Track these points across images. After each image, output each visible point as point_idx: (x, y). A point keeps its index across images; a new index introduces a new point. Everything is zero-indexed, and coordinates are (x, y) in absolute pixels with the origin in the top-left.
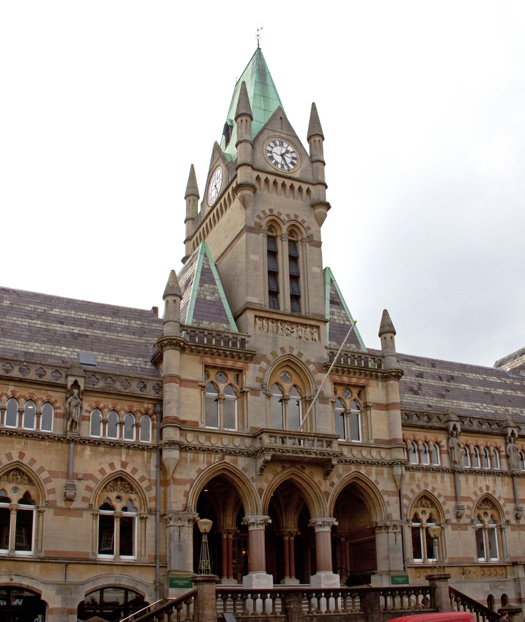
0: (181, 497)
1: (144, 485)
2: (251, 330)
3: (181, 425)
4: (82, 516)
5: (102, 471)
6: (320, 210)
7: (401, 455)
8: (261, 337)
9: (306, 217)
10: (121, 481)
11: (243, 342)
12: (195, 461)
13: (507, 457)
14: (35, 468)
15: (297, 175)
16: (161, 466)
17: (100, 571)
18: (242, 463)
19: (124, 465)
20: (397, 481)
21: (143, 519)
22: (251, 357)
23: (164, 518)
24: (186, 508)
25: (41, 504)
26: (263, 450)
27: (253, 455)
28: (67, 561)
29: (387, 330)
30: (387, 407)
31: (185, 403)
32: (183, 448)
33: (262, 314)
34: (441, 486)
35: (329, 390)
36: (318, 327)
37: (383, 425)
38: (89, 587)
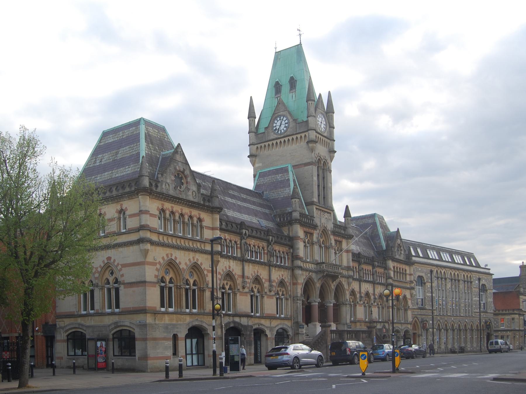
0: (299, 290)
1: (288, 284)
2: (315, 215)
3: (300, 259)
4: (247, 296)
5: (277, 278)
6: (332, 155)
7: (351, 273)
8: (320, 219)
10: (282, 283)
11: (313, 220)
12: (303, 274)
13: (373, 274)
14: (261, 277)
16: (294, 276)
17: (279, 322)
18: (314, 276)
19: (282, 275)
20: (349, 284)
21: (287, 299)
22: (315, 227)
23: (295, 299)
24: (301, 295)
25: (264, 293)
26: (323, 271)
27: (316, 272)
28: (271, 318)
30: (347, 251)
31: (301, 249)
33: (318, 207)
36: (330, 213)
37: (346, 260)
38: (277, 328)
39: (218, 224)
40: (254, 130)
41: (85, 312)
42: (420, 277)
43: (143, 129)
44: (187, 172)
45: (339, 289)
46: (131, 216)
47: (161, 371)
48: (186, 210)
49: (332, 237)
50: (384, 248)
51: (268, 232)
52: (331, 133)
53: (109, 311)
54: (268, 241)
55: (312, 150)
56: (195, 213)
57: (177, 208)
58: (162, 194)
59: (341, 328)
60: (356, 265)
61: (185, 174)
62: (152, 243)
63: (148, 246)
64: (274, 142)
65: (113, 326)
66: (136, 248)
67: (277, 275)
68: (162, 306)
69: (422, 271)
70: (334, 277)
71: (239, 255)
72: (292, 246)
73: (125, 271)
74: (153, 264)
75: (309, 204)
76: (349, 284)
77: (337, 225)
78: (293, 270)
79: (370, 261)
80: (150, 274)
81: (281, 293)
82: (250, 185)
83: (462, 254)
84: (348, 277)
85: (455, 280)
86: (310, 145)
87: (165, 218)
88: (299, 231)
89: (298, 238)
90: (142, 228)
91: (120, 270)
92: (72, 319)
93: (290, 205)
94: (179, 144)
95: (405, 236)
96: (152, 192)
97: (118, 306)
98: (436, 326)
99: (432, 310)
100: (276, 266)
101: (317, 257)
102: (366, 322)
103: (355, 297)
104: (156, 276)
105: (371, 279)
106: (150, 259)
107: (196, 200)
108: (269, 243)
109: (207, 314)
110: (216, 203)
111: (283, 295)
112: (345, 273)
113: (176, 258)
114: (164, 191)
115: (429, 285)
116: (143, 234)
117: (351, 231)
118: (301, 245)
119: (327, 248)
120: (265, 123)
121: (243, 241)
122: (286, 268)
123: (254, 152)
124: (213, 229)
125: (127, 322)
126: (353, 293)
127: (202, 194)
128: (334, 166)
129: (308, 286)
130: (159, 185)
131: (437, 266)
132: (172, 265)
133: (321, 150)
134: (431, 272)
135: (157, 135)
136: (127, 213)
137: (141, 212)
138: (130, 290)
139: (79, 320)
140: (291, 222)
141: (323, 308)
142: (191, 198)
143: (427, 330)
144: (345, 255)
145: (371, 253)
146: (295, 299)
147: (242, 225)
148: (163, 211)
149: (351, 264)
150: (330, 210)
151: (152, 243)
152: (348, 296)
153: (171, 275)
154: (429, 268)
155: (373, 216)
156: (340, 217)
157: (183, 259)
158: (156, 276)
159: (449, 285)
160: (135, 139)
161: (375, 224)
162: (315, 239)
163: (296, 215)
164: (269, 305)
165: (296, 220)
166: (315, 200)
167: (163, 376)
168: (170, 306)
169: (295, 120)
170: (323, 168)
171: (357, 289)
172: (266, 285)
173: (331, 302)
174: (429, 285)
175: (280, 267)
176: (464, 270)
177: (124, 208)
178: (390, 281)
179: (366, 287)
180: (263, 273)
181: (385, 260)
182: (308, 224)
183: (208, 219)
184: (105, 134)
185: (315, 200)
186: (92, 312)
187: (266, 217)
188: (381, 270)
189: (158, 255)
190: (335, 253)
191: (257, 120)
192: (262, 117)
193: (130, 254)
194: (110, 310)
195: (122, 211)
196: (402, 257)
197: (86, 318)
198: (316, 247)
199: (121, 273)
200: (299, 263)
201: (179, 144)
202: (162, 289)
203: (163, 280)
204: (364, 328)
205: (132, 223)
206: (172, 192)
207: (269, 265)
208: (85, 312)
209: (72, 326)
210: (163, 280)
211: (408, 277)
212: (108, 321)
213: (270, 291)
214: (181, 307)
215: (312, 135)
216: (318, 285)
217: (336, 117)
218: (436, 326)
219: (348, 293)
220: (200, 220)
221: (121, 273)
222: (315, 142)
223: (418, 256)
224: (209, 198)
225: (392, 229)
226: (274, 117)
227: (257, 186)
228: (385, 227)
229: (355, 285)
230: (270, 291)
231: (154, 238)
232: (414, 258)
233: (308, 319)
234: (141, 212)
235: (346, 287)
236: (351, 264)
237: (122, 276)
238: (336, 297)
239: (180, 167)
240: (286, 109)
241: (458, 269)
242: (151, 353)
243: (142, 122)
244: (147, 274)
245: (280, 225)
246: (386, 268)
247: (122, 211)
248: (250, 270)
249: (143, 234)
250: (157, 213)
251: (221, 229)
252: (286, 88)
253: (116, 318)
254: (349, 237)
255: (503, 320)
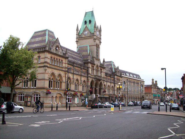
0: (89, 84)
8: (96, 62)
9: (99, 44)
10: (84, 81)
15: (99, 37)
16: (88, 79)
18: (94, 79)
20: (104, 82)
21: (86, 86)
22: (95, 65)
23: (87, 86)
26: (96, 78)
27: (94, 78)
29: (104, 61)
32: (90, 77)
34: (105, 83)
35: (100, 69)
37: (103, 75)
39: (67, 62)
40: (78, 34)
41: (24, 87)
42: (124, 81)
43: (47, 33)
44: (59, 46)
45: (101, 84)
46: (42, 58)
47: (50, 108)
48: (58, 58)
49: (99, 68)
50: (114, 72)
51: (81, 65)
52: (100, 37)
53: (32, 87)
54: (81, 68)
55: (95, 41)
56: (61, 58)
57: (56, 57)
58: (52, 52)
59: (101, 96)
60: (106, 77)
61: (58, 46)
62: (48, 67)
63: (46, 68)
64: (84, 38)
65: (33, 92)
66: (43, 68)
67: (83, 79)
68: (49, 87)
69: (125, 80)
70: (100, 80)
71: (72, 72)
72: (88, 70)
73: (39, 75)
74: (48, 74)
75: (93, 57)
76: (104, 82)
77: (101, 64)
78: (87, 77)
79: (110, 76)
80: (47, 76)
81: (84, 84)
82: (75, 50)
83: (136, 75)
84: (104, 80)
85: (134, 83)
86: (94, 40)
87: (52, 60)
88: (90, 65)
89: (90, 68)
90: (45, 62)
91: (37, 75)
92: (20, 89)
93: (88, 57)
94: (58, 38)
95: (120, 68)
96: (49, 52)
97: (35, 86)
98: (128, 97)
99: (127, 92)
100: (83, 76)
101: (95, 74)
102: (108, 95)
103: (105, 87)
104: (48, 77)
105: (110, 81)
106: (47, 72)
107: (61, 55)
108: (81, 69)
109: (62, 90)
110: (67, 56)
111: (84, 85)
112: (103, 79)
113: (54, 72)
114: (52, 52)
115: (126, 84)
116: (45, 64)
117: (105, 66)
118: (90, 70)
119: (98, 71)
120: (81, 32)
121: (74, 68)
122: (85, 77)
123: (77, 41)
124: (66, 63)
125: (38, 91)
126: (105, 85)
127: (63, 53)
128: (101, 46)
129: (92, 82)
130: (51, 49)
131: (129, 78)
132: (53, 74)
133: (97, 42)
134: (127, 80)
135: (51, 34)
136: (41, 57)
137: (46, 57)
138: (40, 81)
139: (22, 90)
140: (88, 63)
141: (96, 90)
142: (60, 54)
143: (126, 98)
144: (103, 73)
145: (110, 73)
146: (87, 86)
147: (74, 63)
148: (52, 57)
149: (105, 76)
150: (99, 60)
151: (48, 67)
152: (103, 86)
153: (53, 77)
154: (127, 79)
155: (111, 62)
156: (102, 62)
157: (56, 73)
158: (48, 77)
159: (132, 84)
160: (45, 35)
161: (111, 65)
162: (95, 68)
163: (89, 61)
164: (80, 88)
165: (89, 62)
166: (95, 56)
167: (51, 109)
168: (51, 87)
169: (90, 32)
170: (98, 47)
171: (106, 84)
172: (80, 82)
173: (98, 89)
174: (126, 84)
175: (84, 76)
176: (136, 80)
177: (40, 56)
178: (116, 82)
179: (109, 84)
180: (79, 78)
181: (114, 75)
182: (93, 64)
183: (64, 61)
184: (35, 33)
185: (95, 56)
186: (27, 87)
187: (80, 60)
188: (113, 79)
189: (49, 71)
190: (100, 73)
191: (79, 31)
192: (81, 30)
193: (41, 70)
194: (32, 87)
195: (39, 57)
196: (119, 75)
197: (25, 89)
198: (95, 71)
199: (37, 76)
200: (89, 75)
201: (58, 38)
202: (50, 81)
203: (50, 79)
204: (108, 97)
205: (42, 60)
206: (55, 52)
207: (81, 76)
208: (24, 87)
209: (19, 92)
210: (50, 79)
211: (121, 81)
212: (32, 91)
213: (81, 84)
214: (55, 87)
215: (95, 37)
216: (95, 82)
217: (102, 32)
218: (128, 97)
219: (103, 85)
220: (62, 61)
221: (37, 76)
222: (96, 39)
223: (124, 75)
224: (65, 54)
225: (116, 66)
226: (84, 31)
227: (78, 51)
228: (114, 65)
229: (105, 83)
230: (81, 84)
231: (49, 66)
232: (123, 76)
233: (91, 93)
234: (46, 57)
235: (103, 83)
236: (105, 76)
237: (38, 76)
238: (100, 86)
239: (57, 44)
240: (88, 29)
241: (135, 79)
242: (45, 102)
243: (47, 30)
244: (46, 77)
245: (85, 63)
246: (114, 78)
247: (39, 57)
248: (76, 77)
249: (45, 64)
250: (50, 58)
251: (68, 64)
252: (88, 23)
253: (35, 90)
254: (104, 68)
255: (147, 96)
